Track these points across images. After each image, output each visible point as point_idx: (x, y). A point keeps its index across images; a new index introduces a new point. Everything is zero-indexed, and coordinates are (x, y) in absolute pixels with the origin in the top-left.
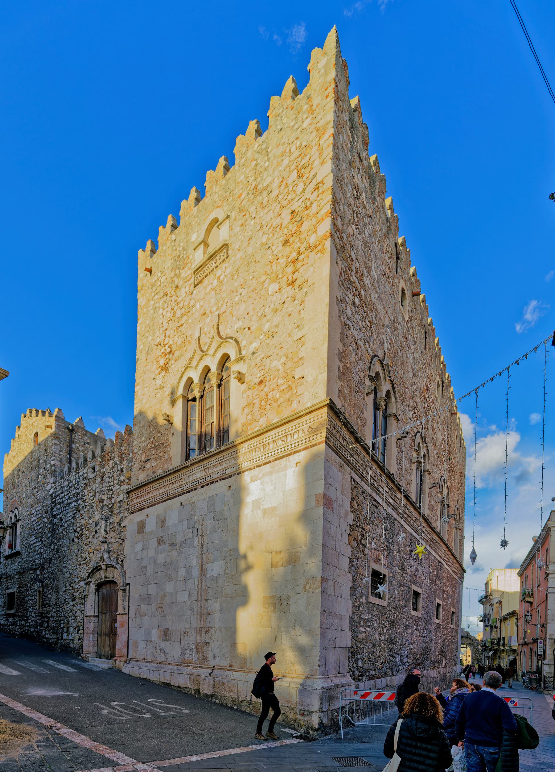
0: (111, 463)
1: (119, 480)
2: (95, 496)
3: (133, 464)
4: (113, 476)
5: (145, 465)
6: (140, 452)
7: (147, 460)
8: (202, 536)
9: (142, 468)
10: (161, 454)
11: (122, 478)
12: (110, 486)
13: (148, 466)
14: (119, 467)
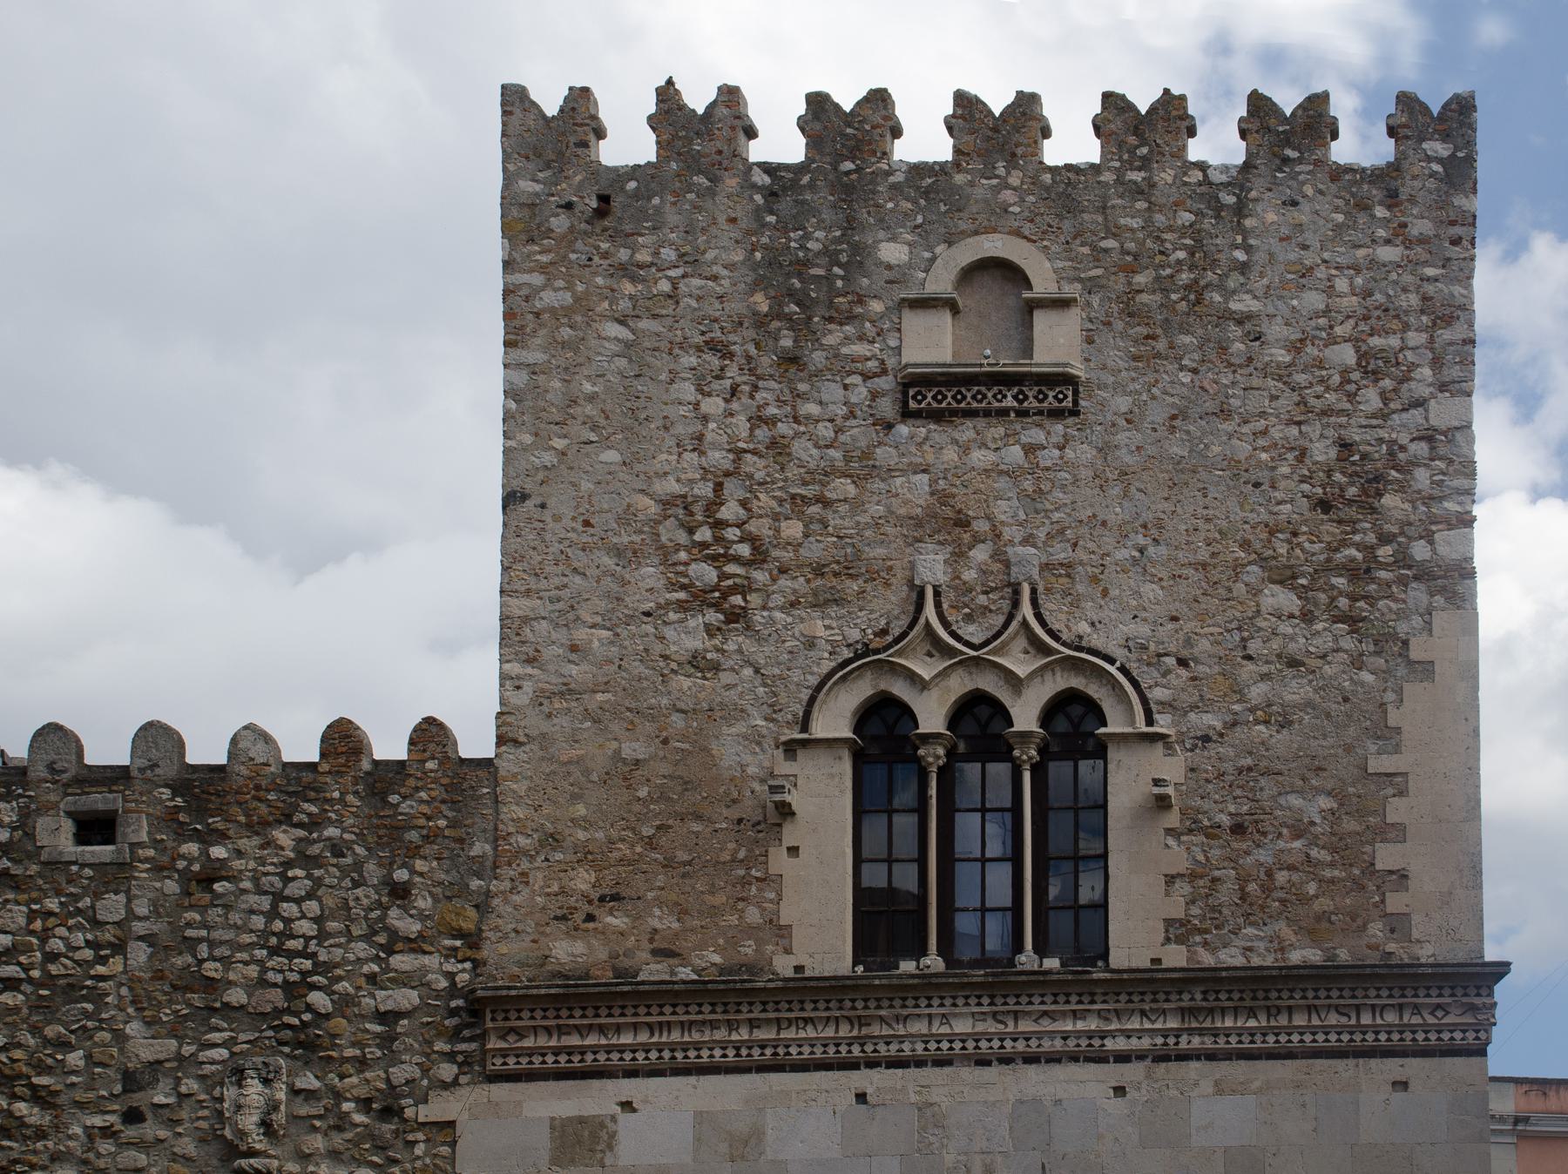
0: (284, 837)
2: (119, 948)
3: (494, 886)
4: (310, 895)
5: (596, 913)
6: (559, 856)
7: (616, 898)
10: (720, 899)
13: (616, 921)
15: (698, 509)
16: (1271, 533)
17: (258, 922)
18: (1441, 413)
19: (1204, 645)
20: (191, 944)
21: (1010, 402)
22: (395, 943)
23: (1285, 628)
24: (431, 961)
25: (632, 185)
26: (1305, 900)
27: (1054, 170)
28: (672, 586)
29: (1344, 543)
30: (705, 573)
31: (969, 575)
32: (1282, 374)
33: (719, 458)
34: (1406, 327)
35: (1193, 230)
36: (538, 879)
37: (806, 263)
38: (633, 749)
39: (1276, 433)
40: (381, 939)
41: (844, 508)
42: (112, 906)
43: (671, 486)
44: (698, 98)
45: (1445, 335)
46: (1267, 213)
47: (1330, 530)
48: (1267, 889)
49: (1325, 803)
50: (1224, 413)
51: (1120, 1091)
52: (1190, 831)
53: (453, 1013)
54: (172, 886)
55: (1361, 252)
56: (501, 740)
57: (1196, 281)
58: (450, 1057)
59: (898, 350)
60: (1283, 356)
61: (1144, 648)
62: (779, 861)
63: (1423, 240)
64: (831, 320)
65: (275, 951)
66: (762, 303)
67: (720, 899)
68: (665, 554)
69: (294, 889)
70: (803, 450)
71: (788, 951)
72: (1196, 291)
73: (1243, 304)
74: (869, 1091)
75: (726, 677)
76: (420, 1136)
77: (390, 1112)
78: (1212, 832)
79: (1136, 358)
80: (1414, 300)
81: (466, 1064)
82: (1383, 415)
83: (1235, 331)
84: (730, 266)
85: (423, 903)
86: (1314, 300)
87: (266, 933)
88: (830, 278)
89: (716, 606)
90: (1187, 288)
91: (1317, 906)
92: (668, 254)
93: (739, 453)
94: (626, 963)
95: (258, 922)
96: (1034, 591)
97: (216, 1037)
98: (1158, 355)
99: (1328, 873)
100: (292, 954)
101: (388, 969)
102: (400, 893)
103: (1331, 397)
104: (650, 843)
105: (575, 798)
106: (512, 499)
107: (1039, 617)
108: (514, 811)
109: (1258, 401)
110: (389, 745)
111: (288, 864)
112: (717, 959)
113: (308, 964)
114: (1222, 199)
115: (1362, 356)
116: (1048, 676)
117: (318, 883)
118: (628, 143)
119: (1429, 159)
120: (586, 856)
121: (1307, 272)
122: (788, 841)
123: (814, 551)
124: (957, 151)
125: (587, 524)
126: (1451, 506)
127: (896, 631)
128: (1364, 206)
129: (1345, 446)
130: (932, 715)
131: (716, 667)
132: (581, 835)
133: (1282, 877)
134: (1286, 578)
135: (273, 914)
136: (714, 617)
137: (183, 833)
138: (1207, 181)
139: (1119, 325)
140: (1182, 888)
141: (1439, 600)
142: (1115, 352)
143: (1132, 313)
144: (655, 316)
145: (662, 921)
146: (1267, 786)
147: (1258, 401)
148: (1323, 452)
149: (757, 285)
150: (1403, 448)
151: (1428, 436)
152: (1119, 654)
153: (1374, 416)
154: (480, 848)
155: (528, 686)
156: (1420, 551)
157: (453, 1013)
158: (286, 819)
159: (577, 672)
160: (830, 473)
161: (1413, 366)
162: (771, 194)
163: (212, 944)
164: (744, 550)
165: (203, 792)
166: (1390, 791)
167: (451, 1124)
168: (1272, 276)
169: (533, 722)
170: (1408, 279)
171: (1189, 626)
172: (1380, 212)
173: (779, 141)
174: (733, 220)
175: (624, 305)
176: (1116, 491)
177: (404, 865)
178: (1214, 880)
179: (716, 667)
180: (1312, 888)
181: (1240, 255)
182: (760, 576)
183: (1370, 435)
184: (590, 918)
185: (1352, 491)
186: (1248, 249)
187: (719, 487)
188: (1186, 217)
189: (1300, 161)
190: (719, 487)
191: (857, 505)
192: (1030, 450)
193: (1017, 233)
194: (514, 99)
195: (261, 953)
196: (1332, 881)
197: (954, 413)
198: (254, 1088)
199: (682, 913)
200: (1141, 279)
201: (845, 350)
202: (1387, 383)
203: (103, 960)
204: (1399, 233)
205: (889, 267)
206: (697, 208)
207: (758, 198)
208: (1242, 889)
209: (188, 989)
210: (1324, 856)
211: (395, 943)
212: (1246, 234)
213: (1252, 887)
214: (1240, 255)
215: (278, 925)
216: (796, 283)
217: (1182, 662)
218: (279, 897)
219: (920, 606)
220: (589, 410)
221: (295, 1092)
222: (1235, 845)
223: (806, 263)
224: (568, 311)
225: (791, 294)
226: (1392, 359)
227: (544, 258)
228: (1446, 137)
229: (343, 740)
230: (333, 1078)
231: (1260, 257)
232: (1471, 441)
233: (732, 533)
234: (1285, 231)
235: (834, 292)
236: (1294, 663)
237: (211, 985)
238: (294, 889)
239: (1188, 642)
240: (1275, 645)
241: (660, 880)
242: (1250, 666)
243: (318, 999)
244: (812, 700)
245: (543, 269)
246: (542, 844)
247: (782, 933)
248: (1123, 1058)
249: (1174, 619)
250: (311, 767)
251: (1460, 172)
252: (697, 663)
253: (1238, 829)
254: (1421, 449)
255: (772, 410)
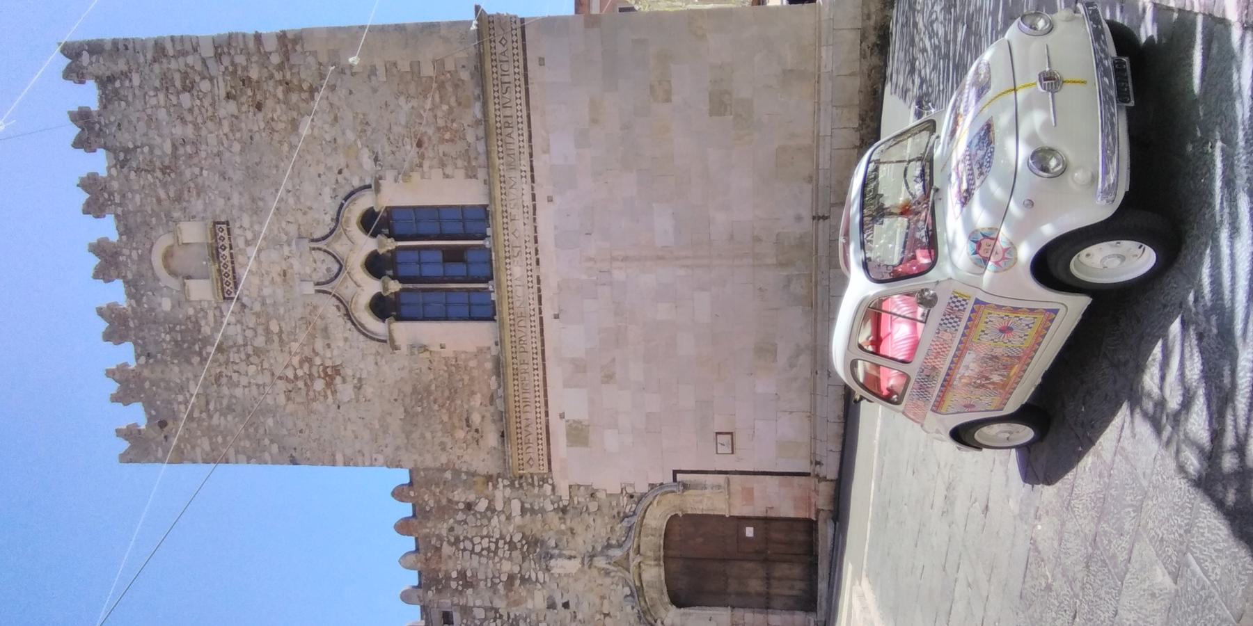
0: (447, 550)
1: (483, 515)
2: (497, 611)
4: (471, 541)
6: (449, 446)
7: (467, 420)
8: (613, 259)
9: (477, 435)
10: (466, 378)
11: (482, 505)
12: (488, 549)
13: (476, 418)
14: (460, 516)
15: (290, 387)
16: (273, 130)
17: (484, 560)
18: (208, 52)
19: (330, 162)
20: (494, 584)
21: (226, 252)
22: (491, 509)
23: (319, 123)
24: (499, 495)
25: (153, 413)
26: (451, 108)
27: (121, 234)
28: (326, 397)
29: (275, 96)
30: (319, 385)
31: (308, 270)
32: (197, 127)
33: (266, 378)
34: (169, 69)
35: (138, 170)
36: (459, 452)
37: (176, 342)
38: (400, 413)
39: (226, 129)
40: (489, 513)
41: (283, 324)
42: (479, 613)
43: (282, 399)
44: (114, 387)
45: (171, 52)
46: (125, 139)
47: (270, 103)
48: (446, 129)
49: (402, 101)
50: (219, 154)
51: (550, 200)
52: (421, 166)
53: (521, 485)
54: (470, 591)
55: (137, 92)
56: (399, 466)
57: (161, 169)
58: (540, 487)
59: (209, 302)
60: (190, 127)
61: (334, 190)
62: (448, 352)
63: (128, 62)
64: (199, 331)
65: (495, 553)
66: (196, 360)
67: (466, 378)
68: (311, 400)
69: (469, 546)
70: (260, 341)
71: (489, 348)
72: (165, 170)
73: (168, 148)
74: (552, 313)
75: (364, 376)
76: (576, 499)
77: (564, 510)
78: (422, 157)
79: (198, 195)
80: (156, 67)
81: (544, 480)
82: (211, 79)
83: (181, 151)
84: (181, 372)
85: (472, 497)
86: (162, 114)
87: (488, 557)
88: (181, 332)
89: (332, 378)
90: (164, 174)
91: (453, 103)
92: (181, 398)
93: (263, 370)
94: (496, 417)
95: (484, 560)
96: (313, 240)
97: (534, 578)
98: (196, 186)
99: (437, 99)
100: (497, 548)
101: (503, 511)
102: (469, 506)
103: (206, 104)
104: (442, 406)
105: (423, 437)
106: (294, 462)
107: (324, 238)
108: (429, 462)
109: (212, 139)
110: (406, 510)
111: (458, 549)
112: (494, 378)
113: (501, 542)
114: (122, 158)
115: (185, 89)
116: (350, 234)
117: (466, 538)
118: (136, 415)
119: (91, 63)
120: (449, 431)
121: (150, 118)
122: (437, 348)
123: (302, 337)
124: (118, 277)
125: (301, 431)
126: (251, 44)
127: (337, 303)
128: (116, 92)
129: (229, 96)
130: (372, 287)
131: (360, 380)
132: (440, 434)
133: (441, 123)
134: (294, 125)
135: (480, 554)
136: (338, 380)
137: (447, 586)
138: (115, 166)
139: (185, 204)
140: (449, 170)
141: (298, 48)
142: (197, 205)
143: (179, 199)
144: (207, 403)
145: (477, 400)
146: (397, 130)
147: (212, 139)
148: (232, 107)
149: (189, 362)
150: (226, 68)
151: (218, 57)
152: (339, 200)
153: (213, 84)
154: (448, 475)
155: (374, 456)
156: (275, 59)
157: (521, 485)
158: (438, 549)
159: (366, 435)
160: (268, 331)
161: (187, 65)
162: (149, 355)
163: (494, 577)
164: (306, 366)
165: (430, 581)
166: (394, 70)
167: (570, 487)
168: (152, 133)
169: (389, 451)
170: (147, 70)
171: (321, 169)
172: (117, 84)
173: (125, 354)
174: (162, 372)
175: (204, 415)
176: (261, 204)
177: (457, 503)
178: (444, 155)
179: (360, 380)
180: (445, 107)
181: (146, 149)
182: (318, 361)
183: (222, 84)
184: (477, 431)
185: (250, 93)
186: (142, 146)
187: (280, 378)
188: (133, 174)
189: (99, 123)
190: (280, 378)
191: (279, 319)
192: (248, 243)
193: (150, 251)
194: (126, 458)
195: (497, 559)
196: (441, 97)
197: (234, 277)
198: (552, 563)
199: (473, 393)
200: (162, 194)
201: (212, 325)
202: (197, 79)
203: (501, 616)
204: (126, 75)
205: (173, 307)
206: (158, 387)
207: (151, 361)
208: (447, 141)
209: (512, 585)
210: (429, 101)
211: (491, 509)
212: (136, 147)
213: (447, 136)
214: (146, 149)
215: (485, 553)
216: (186, 345)
217: (340, 172)
218: (472, 552)
219: (324, 292)
220: (251, 430)
221: (557, 546)
222: (426, 145)
223: (176, 342)
224: (210, 438)
225: (189, 348)
226: (185, 76)
227: (189, 446)
228: (79, 55)
229: (404, 527)
230: (551, 533)
231: (145, 139)
232: (219, 36)
233: (300, 373)
234: (132, 129)
235: (187, 330)
236: (336, 119)
237: (511, 578)
238: (469, 546)
239: (329, 169)
240: (327, 127)
241: (459, 402)
242: (340, 141)
243: (517, 538)
244: (372, 338)
245: (193, 448)
246: (444, 449)
247: (480, 351)
248: (534, 198)
249: (319, 176)
250: (417, 539)
251: (95, 48)
252: (358, 388)
253: (419, 145)
254: (226, 61)
255: (243, 357)
